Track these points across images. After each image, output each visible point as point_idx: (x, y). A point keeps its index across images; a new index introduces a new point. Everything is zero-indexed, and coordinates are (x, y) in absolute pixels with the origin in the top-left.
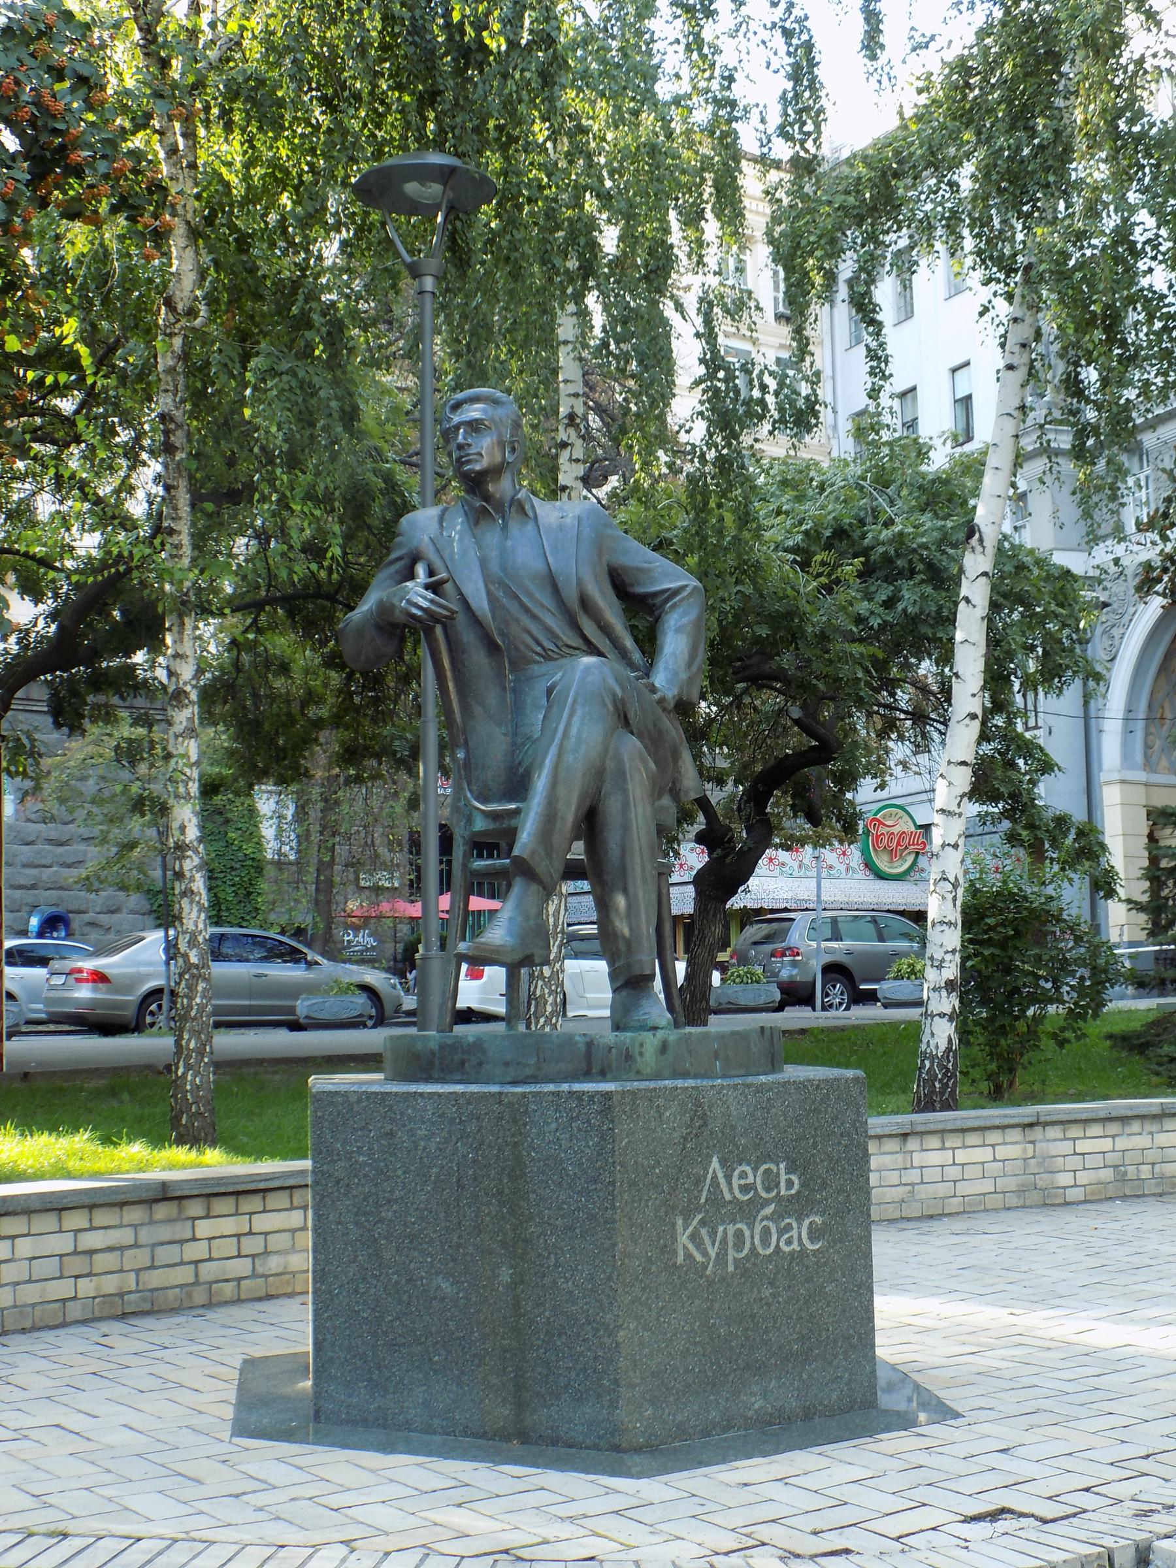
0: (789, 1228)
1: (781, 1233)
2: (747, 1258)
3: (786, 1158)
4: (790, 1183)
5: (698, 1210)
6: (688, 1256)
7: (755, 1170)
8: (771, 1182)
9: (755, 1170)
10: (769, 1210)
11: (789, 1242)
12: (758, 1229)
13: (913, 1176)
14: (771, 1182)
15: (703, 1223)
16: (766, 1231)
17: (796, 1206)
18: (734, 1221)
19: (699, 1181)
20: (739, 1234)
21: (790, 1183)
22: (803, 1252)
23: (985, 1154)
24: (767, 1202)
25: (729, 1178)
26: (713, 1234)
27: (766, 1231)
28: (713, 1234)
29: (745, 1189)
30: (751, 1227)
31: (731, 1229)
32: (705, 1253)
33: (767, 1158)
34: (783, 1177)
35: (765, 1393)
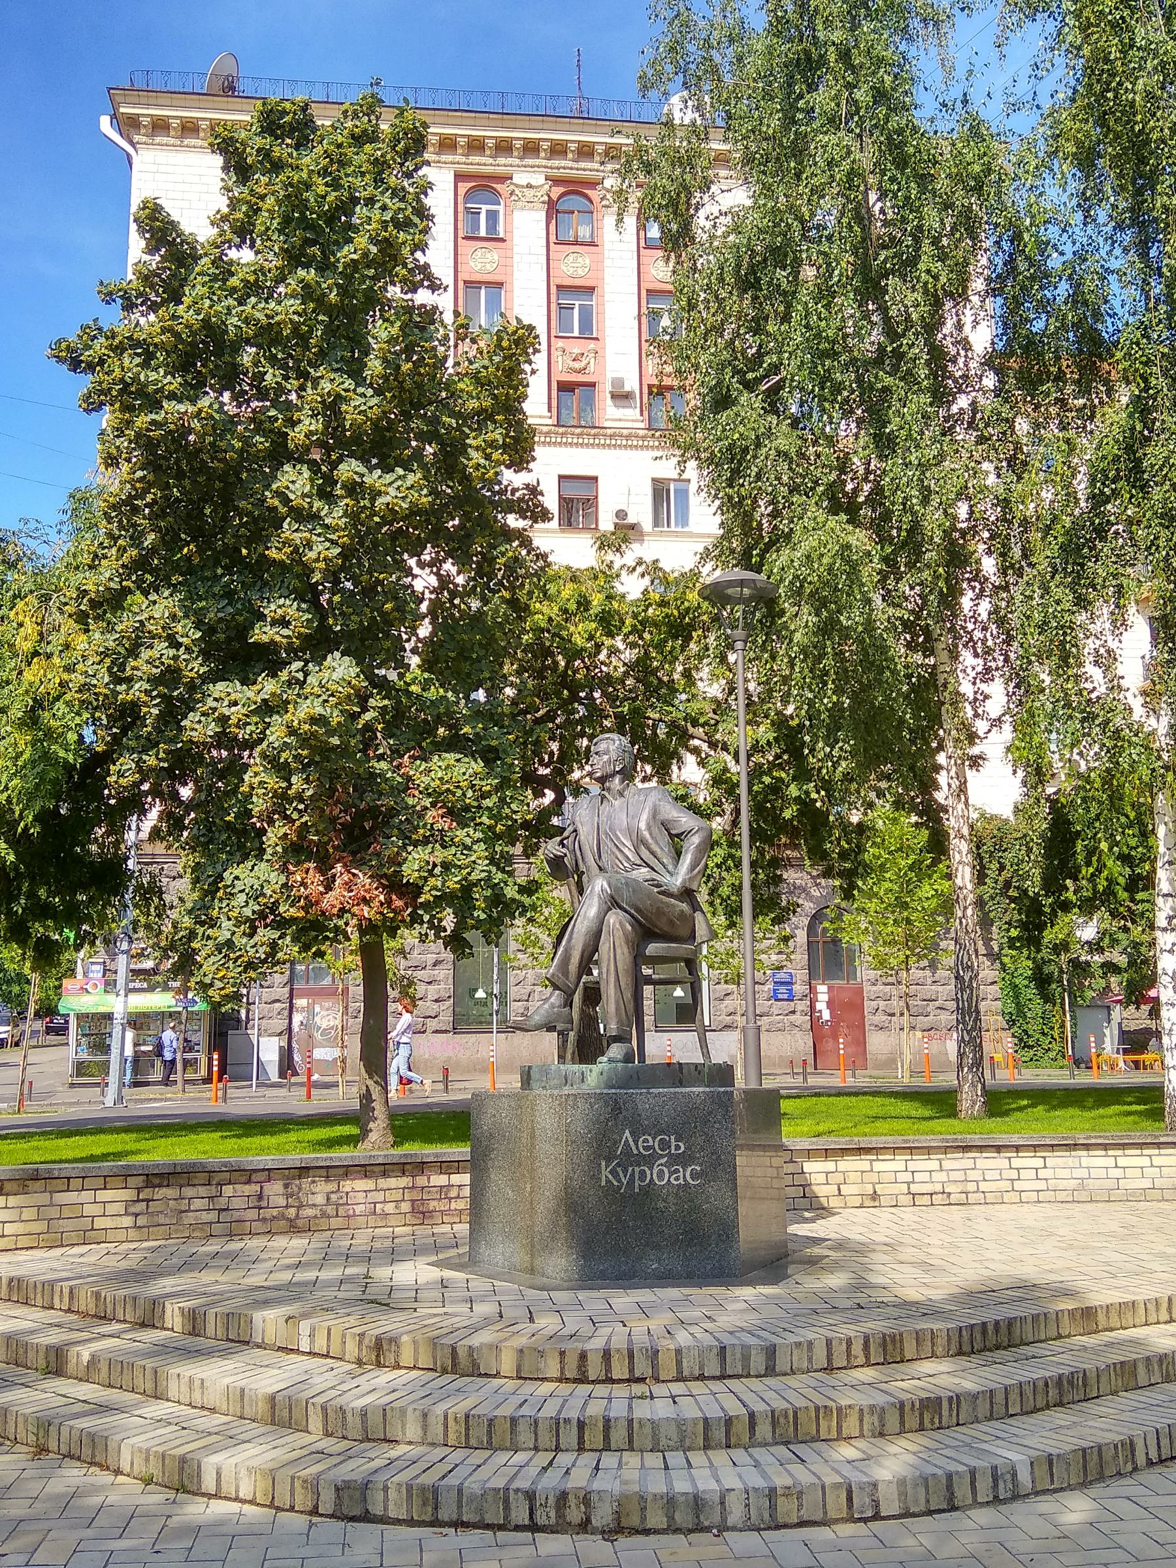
0: (677, 1171)
1: (671, 1173)
2: (649, 1185)
3: (676, 1133)
4: (677, 1147)
5: (616, 1157)
6: (608, 1181)
7: (654, 1139)
8: (665, 1145)
9: (654, 1139)
10: (663, 1161)
11: (677, 1179)
12: (655, 1171)
13: (1083, 1173)
14: (665, 1145)
15: (618, 1165)
16: (661, 1173)
17: (683, 1160)
18: (639, 1165)
19: (616, 1143)
20: (643, 1173)
21: (677, 1147)
22: (687, 1184)
23: (1145, 1161)
24: (662, 1156)
25: (636, 1142)
26: (625, 1172)
27: (661, 1173)
28: (625, 1172)
29: (646, 1148)
30: (651, 1169)
31: (637, 1169)
32: (619, 1181)
33: (662, 1132)
34: (673, 1144)
35: (659, 1261)
